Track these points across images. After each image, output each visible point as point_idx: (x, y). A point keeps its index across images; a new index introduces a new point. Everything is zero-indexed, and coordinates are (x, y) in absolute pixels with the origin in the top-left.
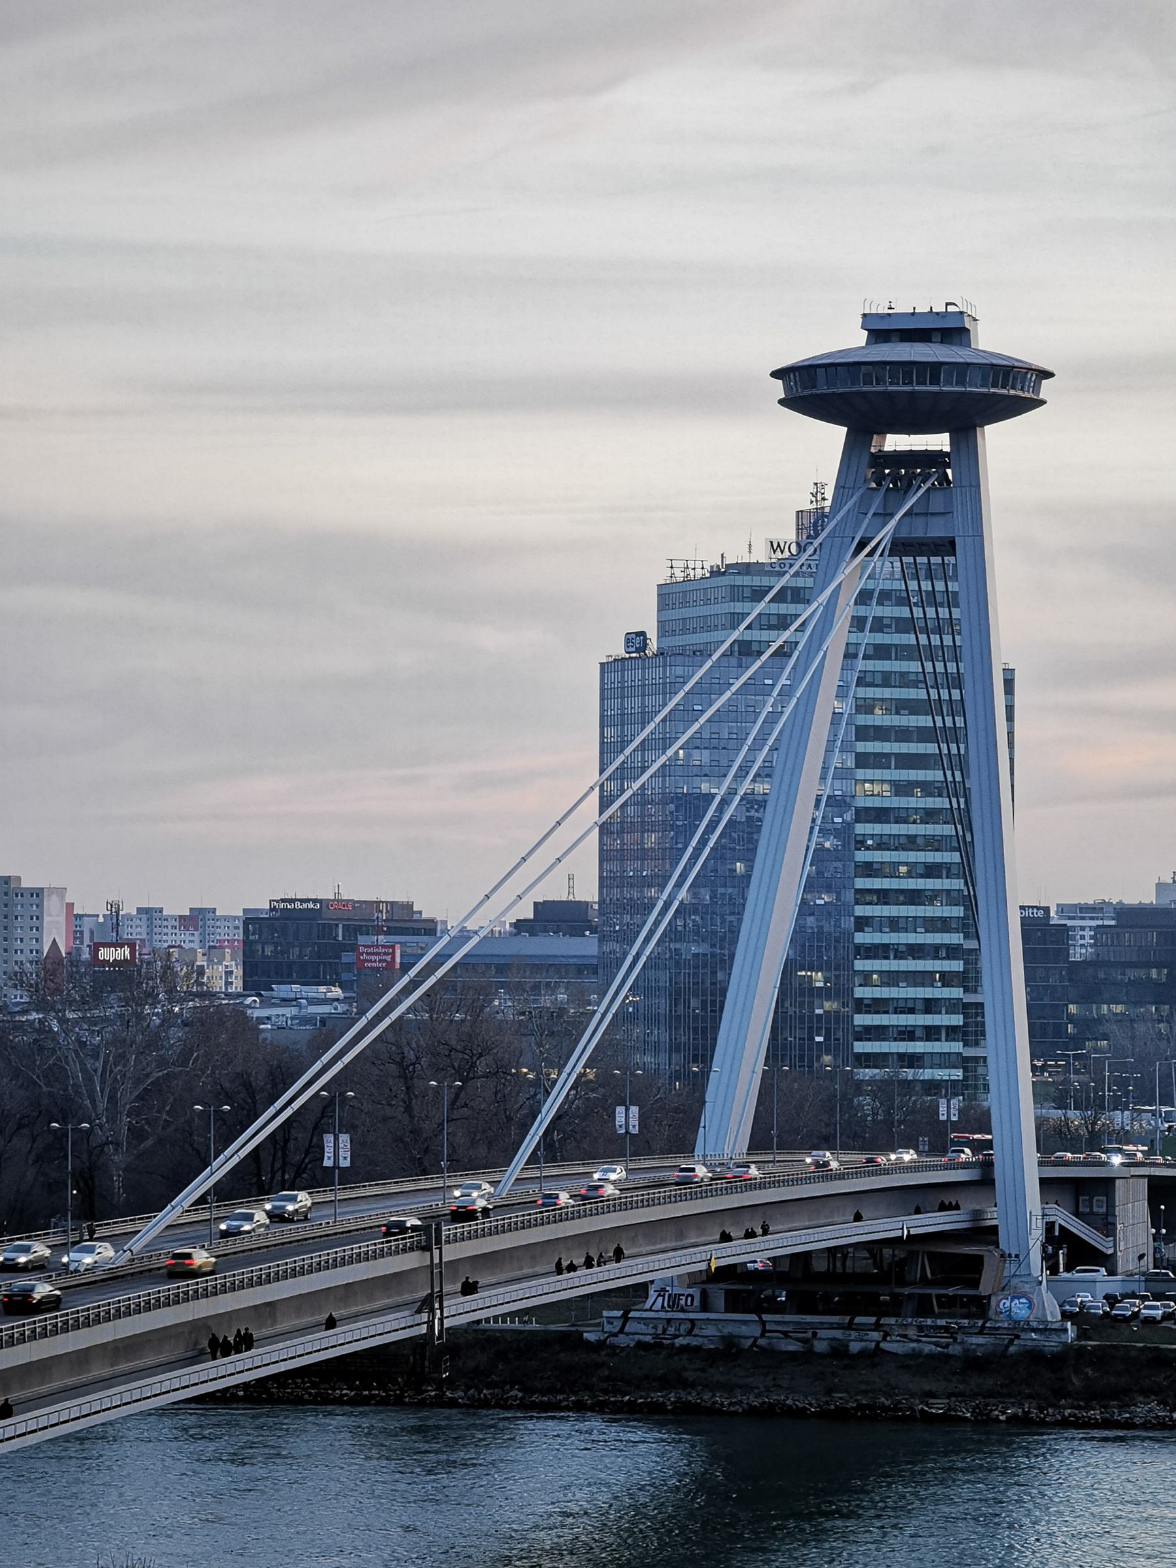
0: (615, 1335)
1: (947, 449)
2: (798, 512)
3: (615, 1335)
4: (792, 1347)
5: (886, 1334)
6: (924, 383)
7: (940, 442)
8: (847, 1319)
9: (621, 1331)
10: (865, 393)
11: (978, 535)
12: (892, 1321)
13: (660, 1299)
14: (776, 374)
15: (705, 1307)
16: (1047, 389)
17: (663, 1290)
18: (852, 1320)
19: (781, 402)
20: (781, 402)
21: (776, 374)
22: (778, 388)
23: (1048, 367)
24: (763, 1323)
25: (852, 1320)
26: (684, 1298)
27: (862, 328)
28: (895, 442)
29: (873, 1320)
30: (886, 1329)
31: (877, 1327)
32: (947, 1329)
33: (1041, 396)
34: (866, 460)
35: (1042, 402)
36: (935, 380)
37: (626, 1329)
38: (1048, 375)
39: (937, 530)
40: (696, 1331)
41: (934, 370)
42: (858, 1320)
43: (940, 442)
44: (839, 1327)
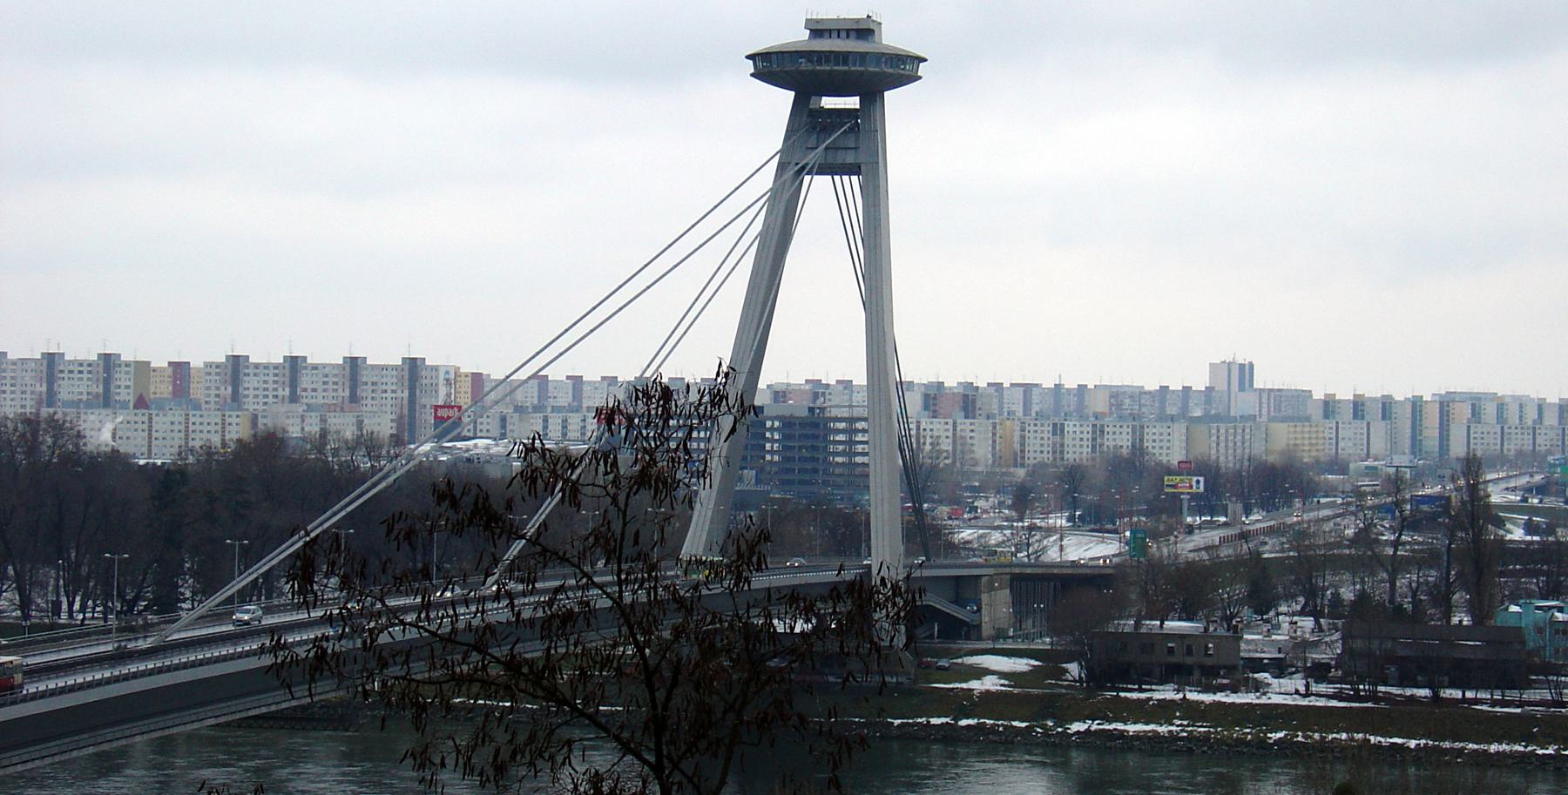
1: (858, 107)
6: (839, 65)
7: (852, 102)
14: (748, 57)
19: (752, 75)
20: (752, 75)
21: (748, 57)
23: (923, 55)
27: (806, 28)
28: (829, 102)
33: (919, 74)
35: (920, 78)
36: (845, 63)
38: (925, 60)
39: (850, 158)
41: (843, 57)
43: (852, 102)
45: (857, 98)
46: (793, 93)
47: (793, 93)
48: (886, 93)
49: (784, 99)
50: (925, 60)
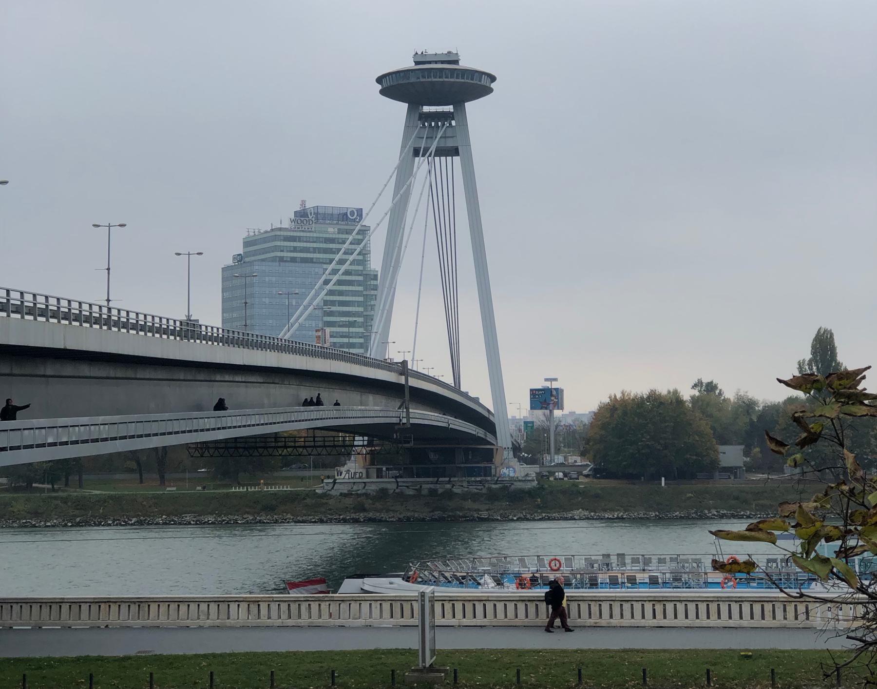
0: (330, 490)
2: (295, 212)
3: (330, 490)
4: (410, 492)
5: (453, 485)
7: (449, 108)
8: (436, 479)
9: (333, 488)
10: (422, 82)
11: (468, 145)
12: (456, 479)
13: (347, 474)
14: (379, 80)
15: (368, 477)
16: (493, 85)
17: (349, 470)
18: (438, 480)
22: (379, 87)
24: (397, 482)
25: (438, 480)
26: (358, 474)
29: (447, 479)
30: (453, 483)
31: (449, 482)
32: (480, 482)
34: (417, 116)
37: (335, 488)
40: (366, 488)
42: (441, 479)
43: (449, 108)
44: (432, 483)
45: (451, 107)
46: (407, 104)
47: (407, 104)
48: (466, 104)
49: (402, 108)
50: (493, 79)
